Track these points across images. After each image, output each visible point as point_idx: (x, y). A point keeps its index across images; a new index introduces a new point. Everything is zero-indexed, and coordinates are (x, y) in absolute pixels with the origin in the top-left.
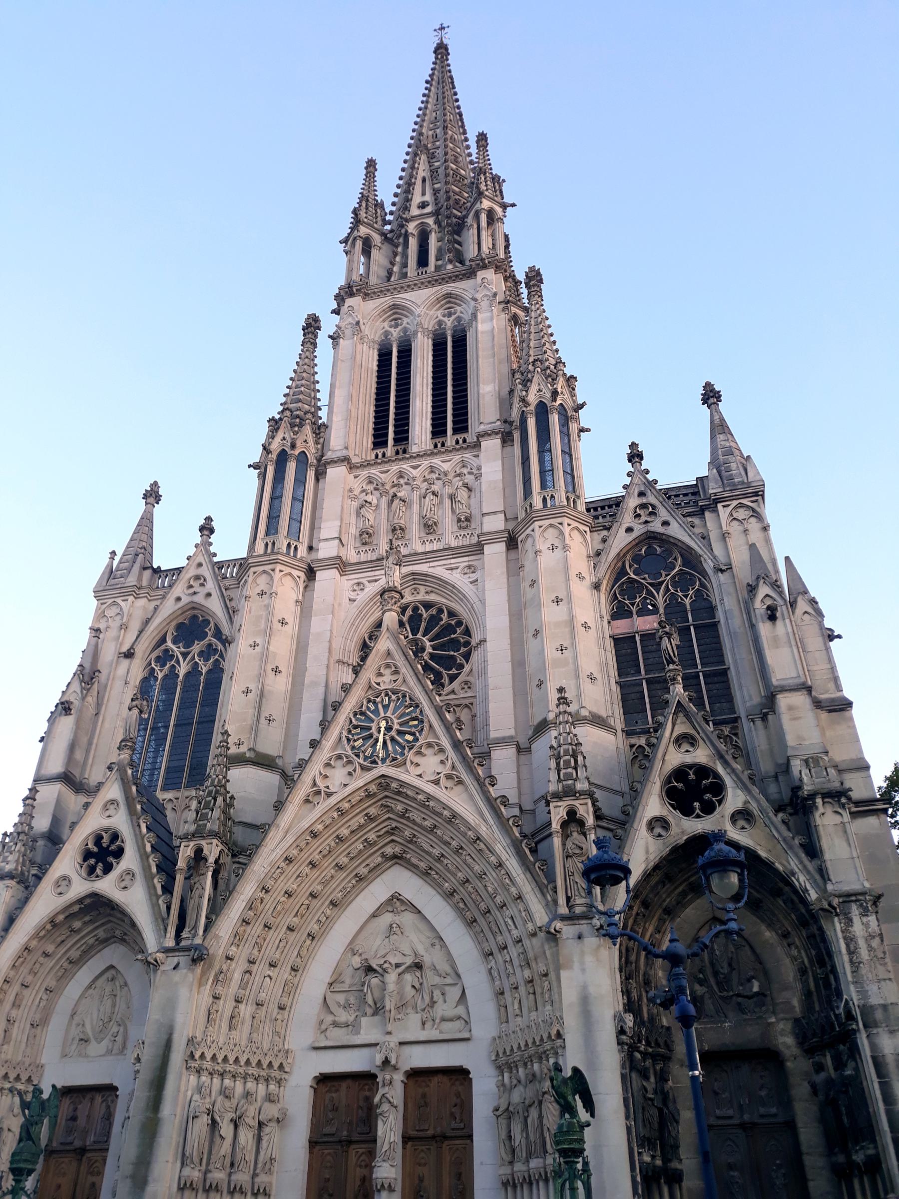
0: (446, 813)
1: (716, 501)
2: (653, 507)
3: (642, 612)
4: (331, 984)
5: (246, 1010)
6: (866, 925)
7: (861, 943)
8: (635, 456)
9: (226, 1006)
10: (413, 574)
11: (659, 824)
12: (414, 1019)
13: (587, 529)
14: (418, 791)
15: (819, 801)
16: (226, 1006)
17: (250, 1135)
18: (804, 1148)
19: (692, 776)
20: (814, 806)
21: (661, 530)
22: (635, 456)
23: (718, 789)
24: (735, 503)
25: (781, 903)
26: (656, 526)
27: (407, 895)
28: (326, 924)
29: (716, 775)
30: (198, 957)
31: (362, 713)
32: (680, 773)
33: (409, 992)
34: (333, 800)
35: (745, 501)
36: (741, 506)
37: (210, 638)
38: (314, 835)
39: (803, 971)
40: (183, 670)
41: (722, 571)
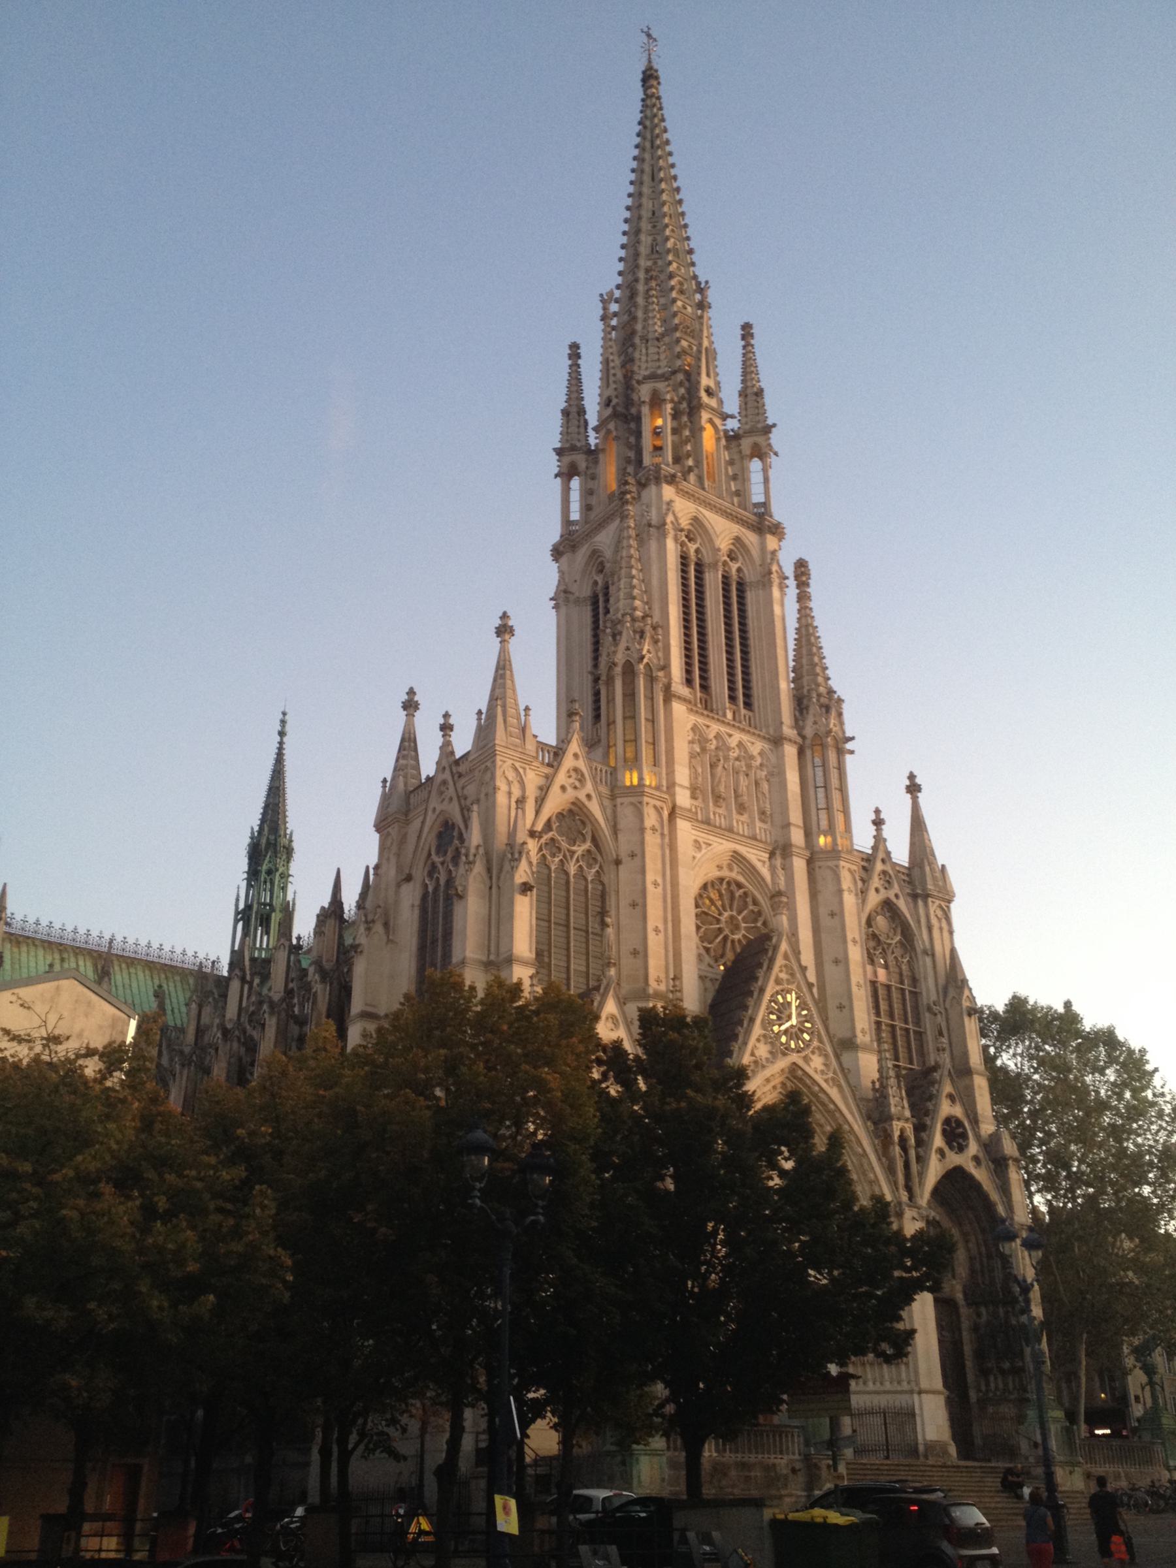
0: (832, 1106)
2: (890, 877)
8: (878, 823)
10: (735, 852)
11: (941, 1152)
14: (815, 1082)
15: (1010, 1162)
18: (966, 1357)
19: (954, 1125)
20: (1007, 1166)
21: (894, 900)
22: (878, 823)
23: (964, 1136)
24: (937, 902)
25: (971, 1216)
29: (964, 1128)
32: (948, 1121)
35: (943, 904)
36: (940, 906)
37: (588, 845)
39: (971, 1259)
40: (572, 869)
41: (928, 954)
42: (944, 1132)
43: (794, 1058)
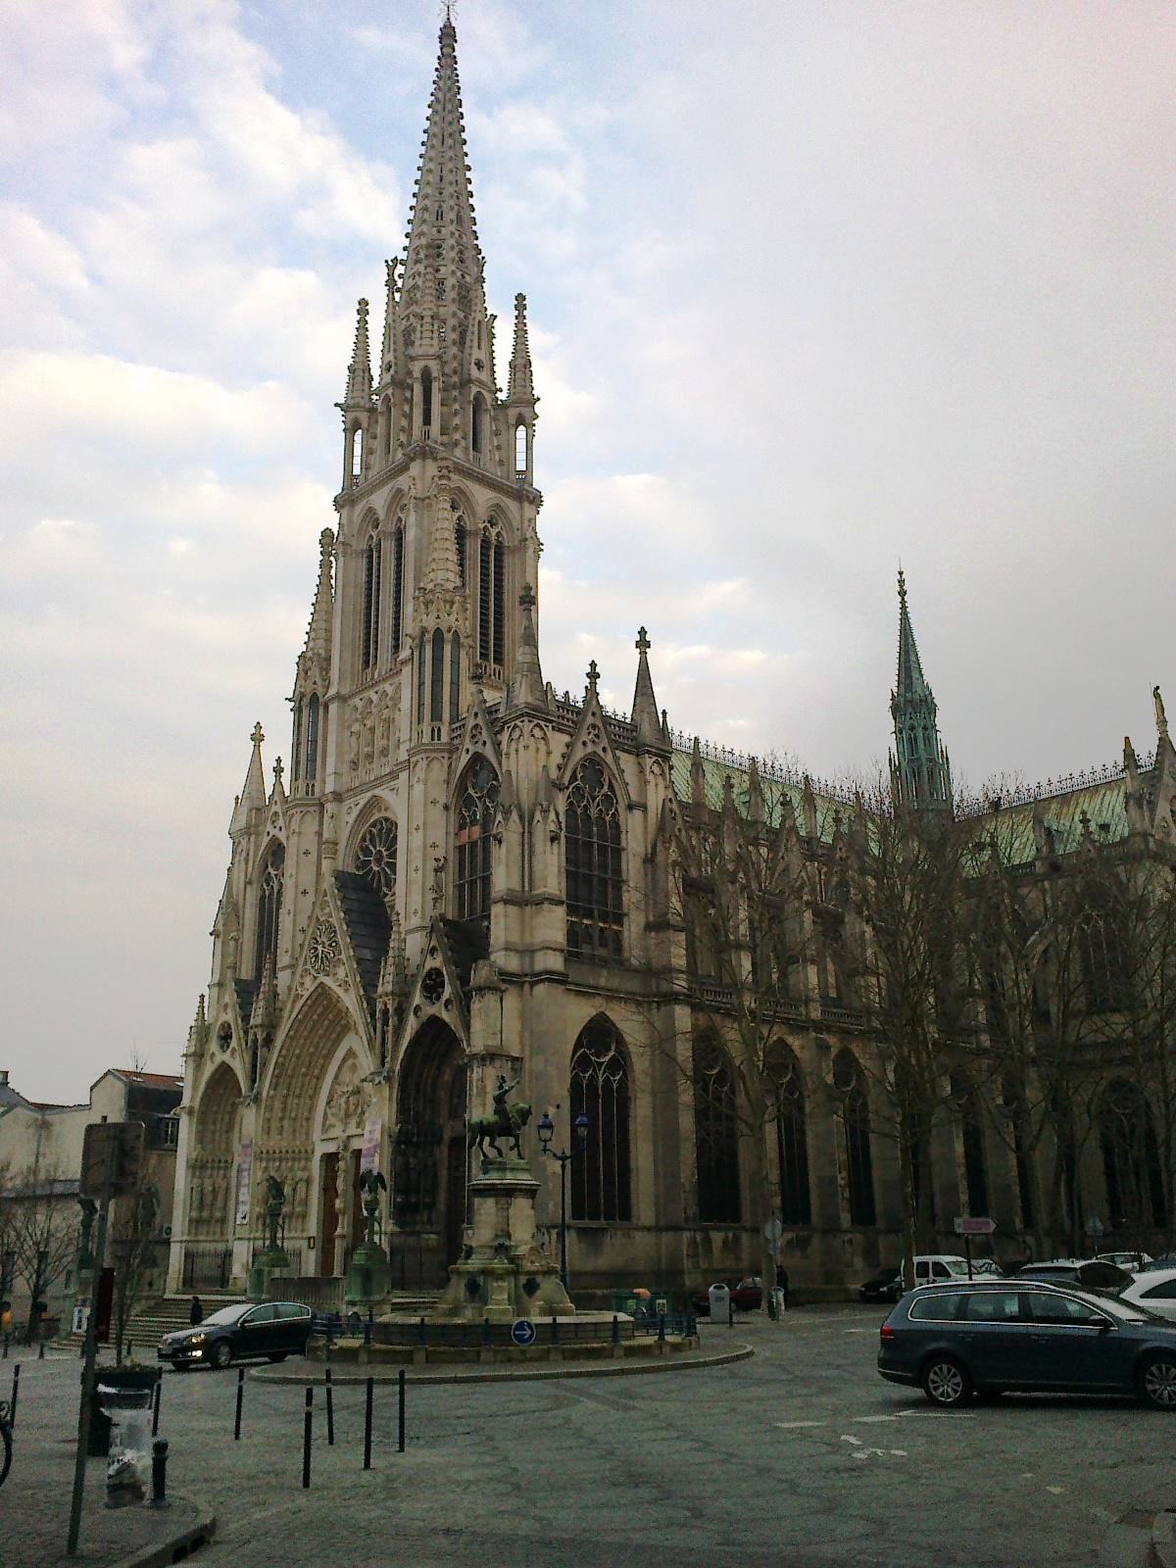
1: (505, 723)
3: (474, 822)
4: (328, 1103)
5: (286, 1123)
6: (477, 1072)
7: (475, 1084)
9: (275, 1125)
12: (353, 1122)
13: (446, 755)
16: (275, 1125)
17: (291, 1188)
26: (479, 748)
27: (354, 1048)
28: (323, 1069)
30: (257, 1099)
31: (315, 939)
33: (352, 1108)
34: (304, 998)
35: (518, 722)
36: (516, 726)
38: (301, 1022)
42: (426, 988)
43: (322, 978)
